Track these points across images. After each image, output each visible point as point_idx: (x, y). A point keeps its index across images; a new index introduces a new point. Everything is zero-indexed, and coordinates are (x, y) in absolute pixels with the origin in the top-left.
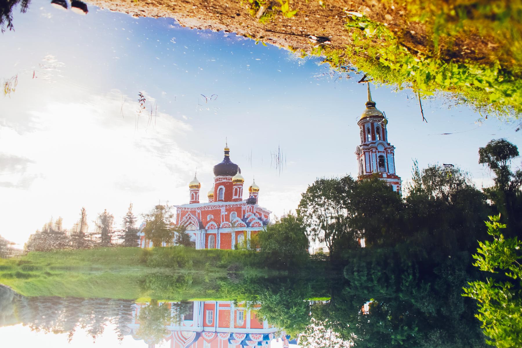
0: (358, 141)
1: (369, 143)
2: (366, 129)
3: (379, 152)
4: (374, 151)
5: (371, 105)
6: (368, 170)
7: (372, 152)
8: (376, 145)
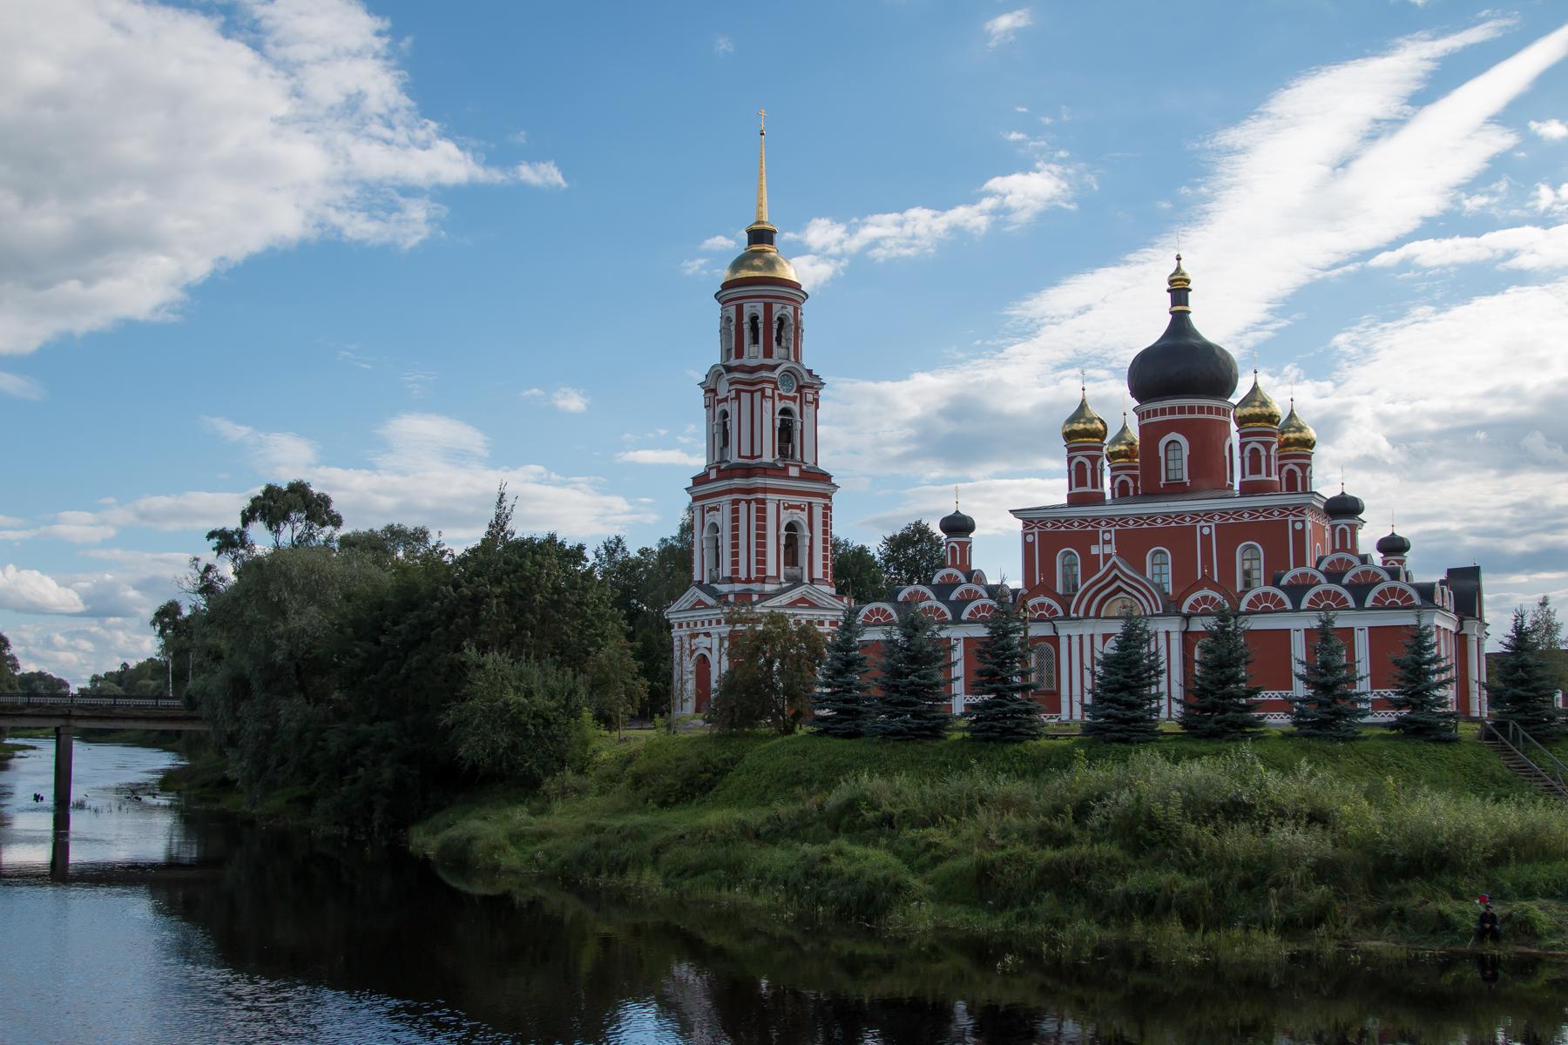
0: (712, 354)
1: (753, 363)
2: (746, 319)
3: (781, 397)
4: (769, 392)
6: (746, 451)
7: (763, 396)
8: (776, 374)
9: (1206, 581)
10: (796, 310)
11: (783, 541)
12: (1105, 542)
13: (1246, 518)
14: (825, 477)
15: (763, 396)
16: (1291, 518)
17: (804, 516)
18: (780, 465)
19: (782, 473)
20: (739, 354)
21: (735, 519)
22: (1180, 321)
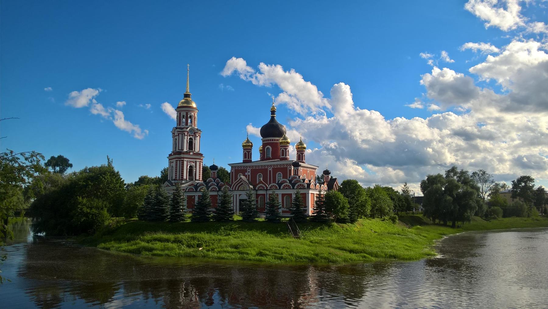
2: (182, 116)
6: (180, 148)
9: (260, 182)
14: (201, 155)
17: (194, 164)
20: (180, 125)
21: (176, 165)
22: (273, 118)
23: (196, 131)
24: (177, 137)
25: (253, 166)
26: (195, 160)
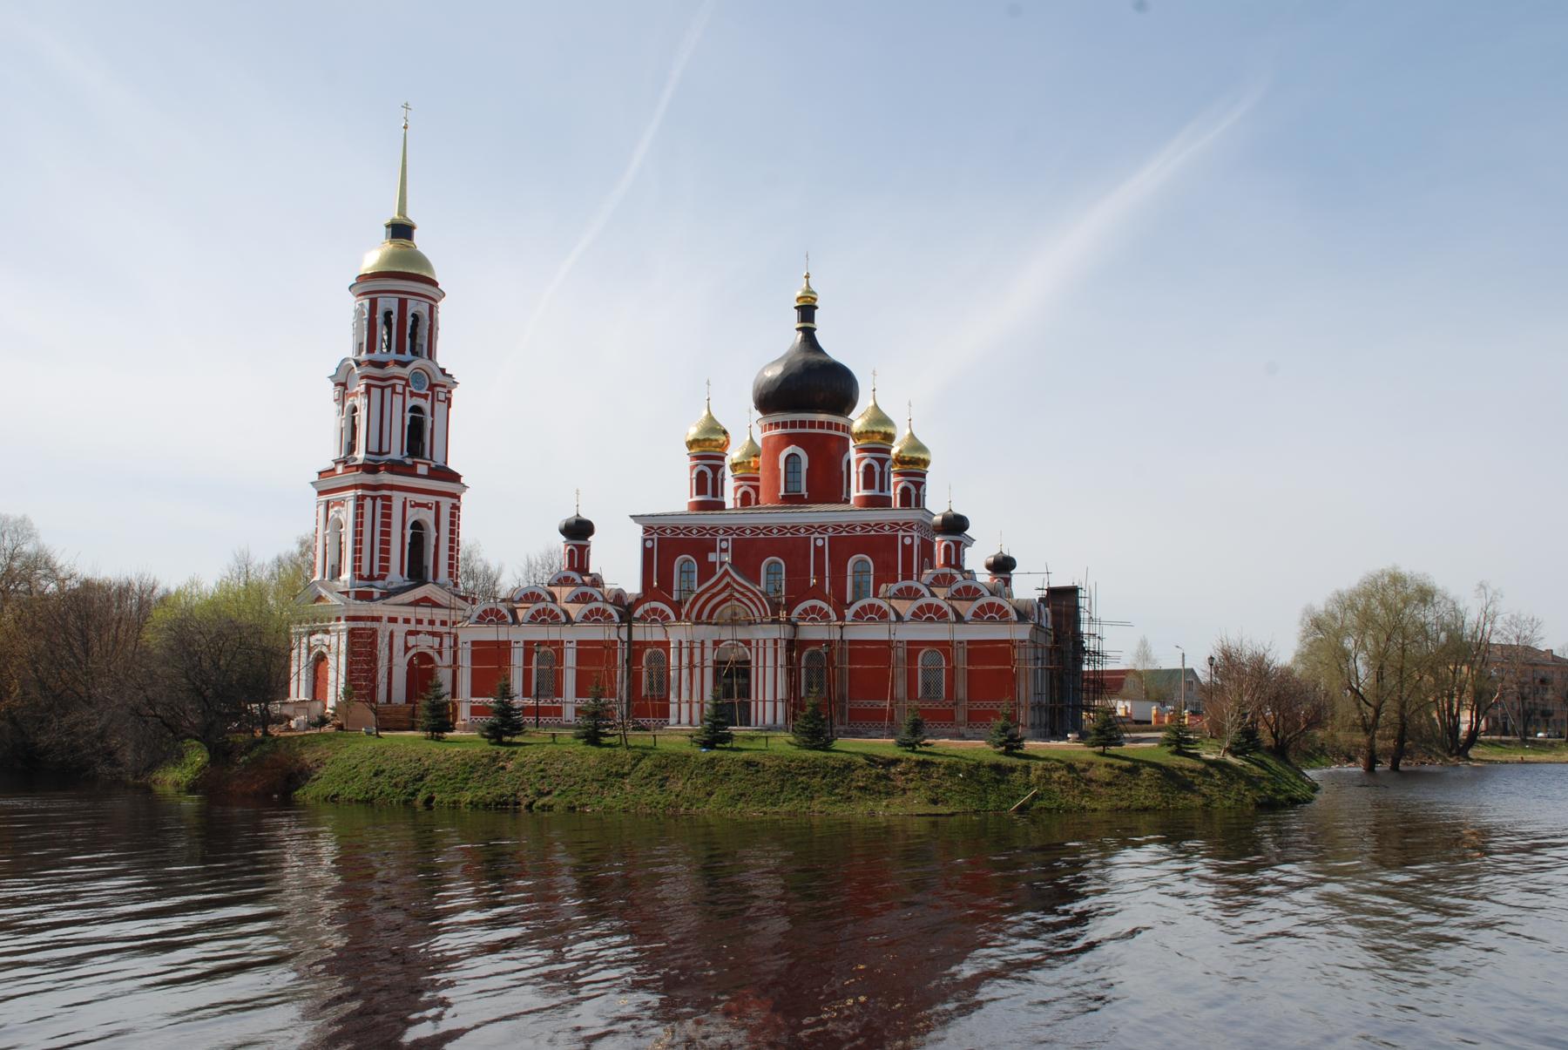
4: (399, 389)
5: (401, 231)
7: (394, 392)
9: (817, 593)
10: (432, 309)
11: (408, 540)
12: (722, 550)
13: (858, 532)
14: (455, 477)
15: (394, 392)
16: (901, 533)
18: (409, 461)
19: (410, 471)
21: (359, 515)
23: (440, 379)
24: (360, 402)
25: (742, 529)
26: (431, 499)
